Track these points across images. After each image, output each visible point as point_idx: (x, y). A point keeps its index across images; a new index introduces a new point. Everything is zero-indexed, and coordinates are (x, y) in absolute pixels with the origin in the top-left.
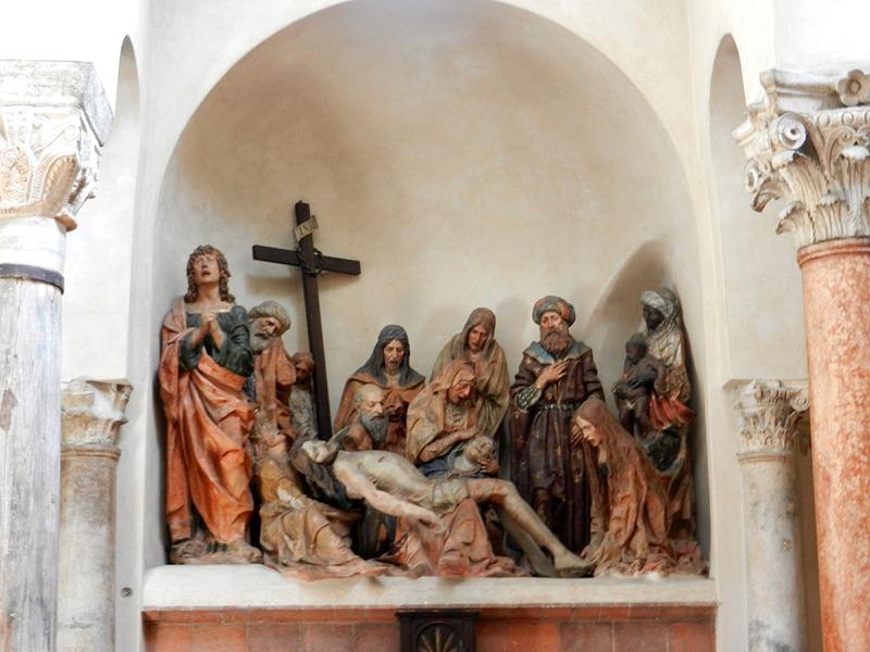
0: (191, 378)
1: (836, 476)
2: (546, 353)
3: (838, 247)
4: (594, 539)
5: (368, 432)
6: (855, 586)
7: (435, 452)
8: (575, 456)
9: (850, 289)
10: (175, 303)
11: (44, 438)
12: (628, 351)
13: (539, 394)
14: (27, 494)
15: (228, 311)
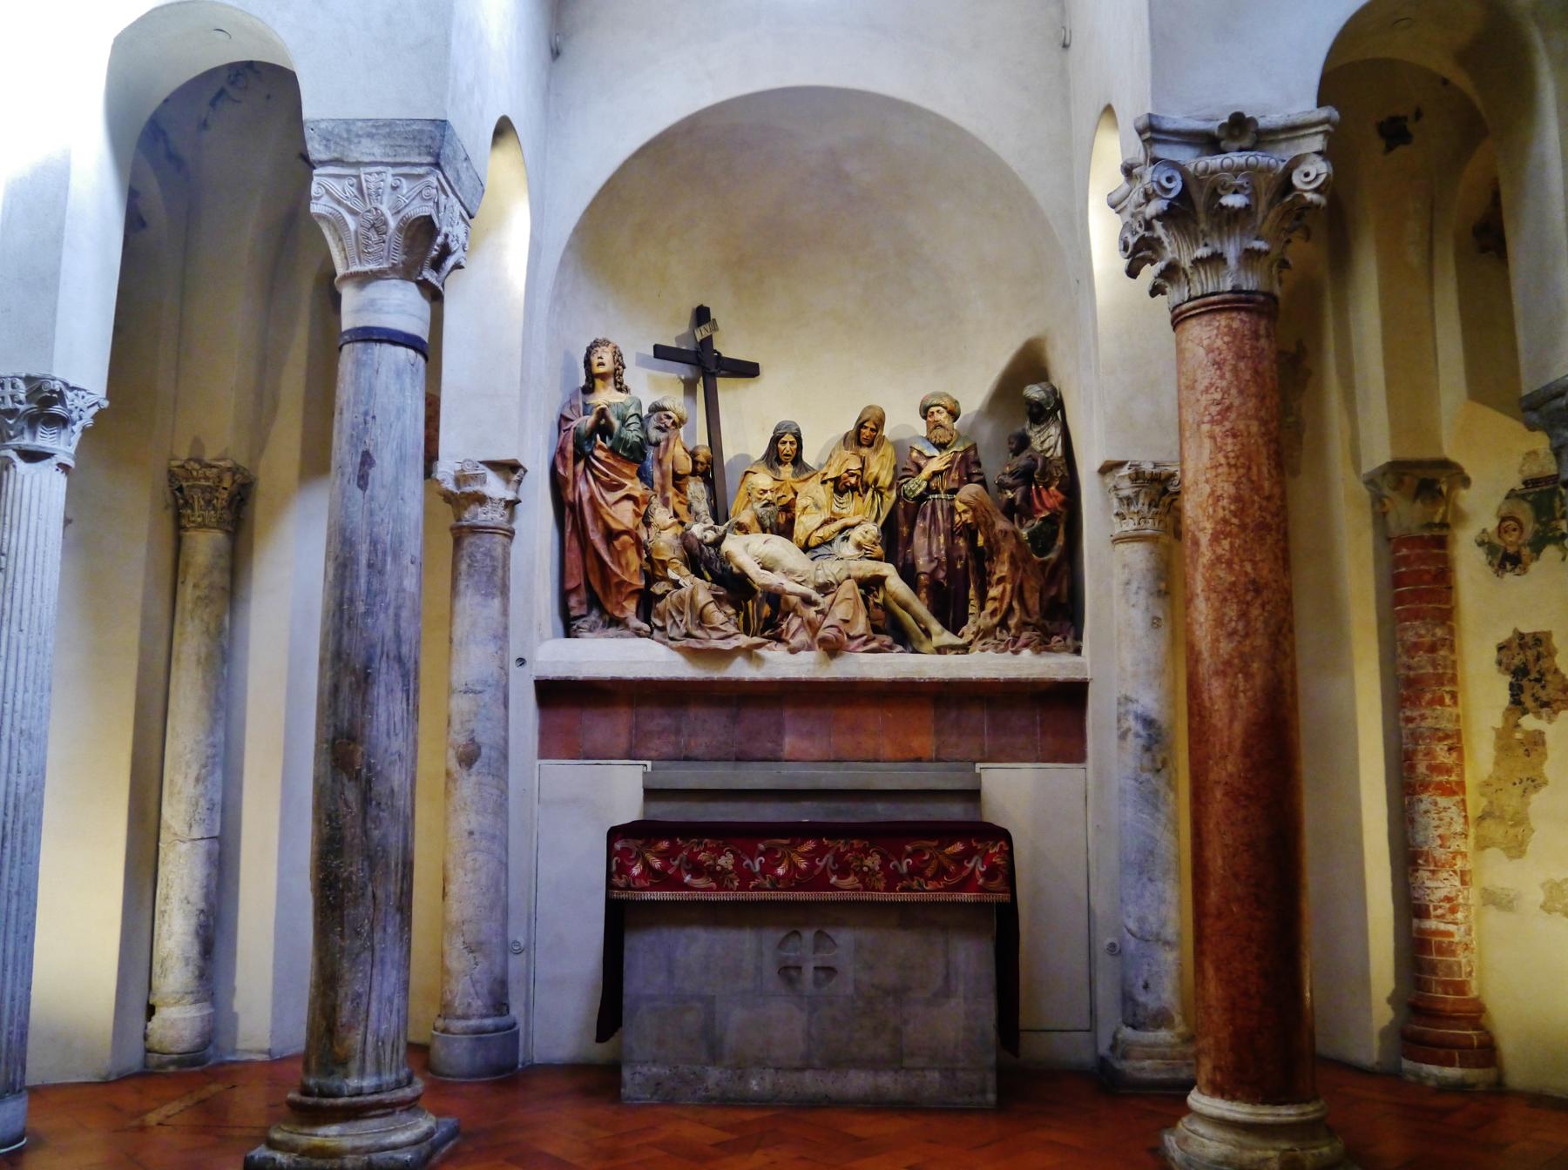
2: (932, 447)
3: (1214, 303)
4: (971, 619)
5: (759, 520)
6: (1221, 651)
8: (958, 543)
9: (1225, 347)
10: (574, 395)
11: (402, 499)
12: (1010, 443)
13: (924, 484)
14: (384, 553)
15: (622, 401)
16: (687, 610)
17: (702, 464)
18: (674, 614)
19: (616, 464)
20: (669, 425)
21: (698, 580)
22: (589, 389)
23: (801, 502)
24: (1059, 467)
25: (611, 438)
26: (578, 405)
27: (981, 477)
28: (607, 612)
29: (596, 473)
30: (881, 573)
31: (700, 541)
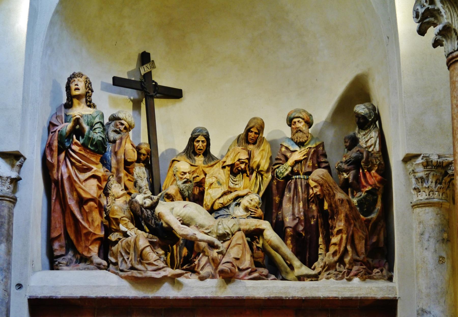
4: (320, 257)
5: (181, 192)
7: (222, 204)
8: (312, 208)
10: (59, 109)
12: (345, 142)
13: (290, 169)
15: (91, 113)
16: (132, 252)
17: (144, 155)
18: (123, 254)
19: (86, 155)
20: (122, 129)
21: (140, 232)
22: (69, 106)
23: (208, 181)
24: (377, 158)
25: (83, 138)
26: (62, 116)
27: (327, 164)
28: (79, 254)
29: (73, 160)
30: (260, 227)
31: (142, 206)
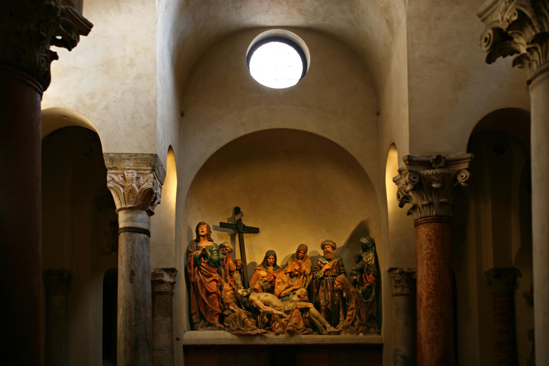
0: (198, 268)
1: (424, 299)
4: (341, 322)
5: (262, 287)
8: (335, 295)
13: (323, 274)
15: (211, 245)
16: (238, 320)
17: (239, 266)
18: (233, 322)
19: (209, 268)
20: (227, 252)
21: (241, 310)
22: (198, 240)
23: (277, 280)
25: (207, 258)
26: (194, 247)
28: (207, 321)
30: (308, 307)
31: (241, 296)
